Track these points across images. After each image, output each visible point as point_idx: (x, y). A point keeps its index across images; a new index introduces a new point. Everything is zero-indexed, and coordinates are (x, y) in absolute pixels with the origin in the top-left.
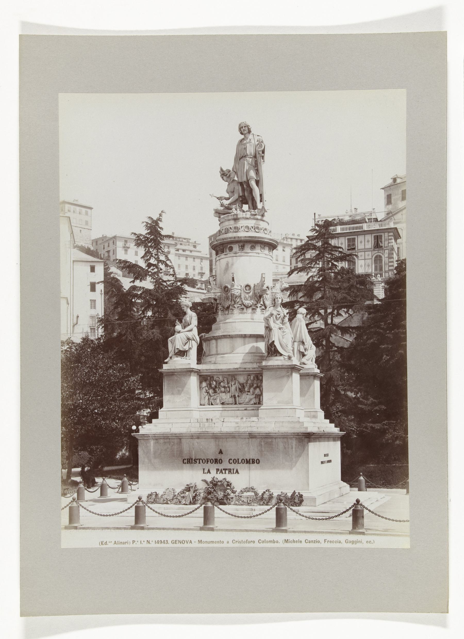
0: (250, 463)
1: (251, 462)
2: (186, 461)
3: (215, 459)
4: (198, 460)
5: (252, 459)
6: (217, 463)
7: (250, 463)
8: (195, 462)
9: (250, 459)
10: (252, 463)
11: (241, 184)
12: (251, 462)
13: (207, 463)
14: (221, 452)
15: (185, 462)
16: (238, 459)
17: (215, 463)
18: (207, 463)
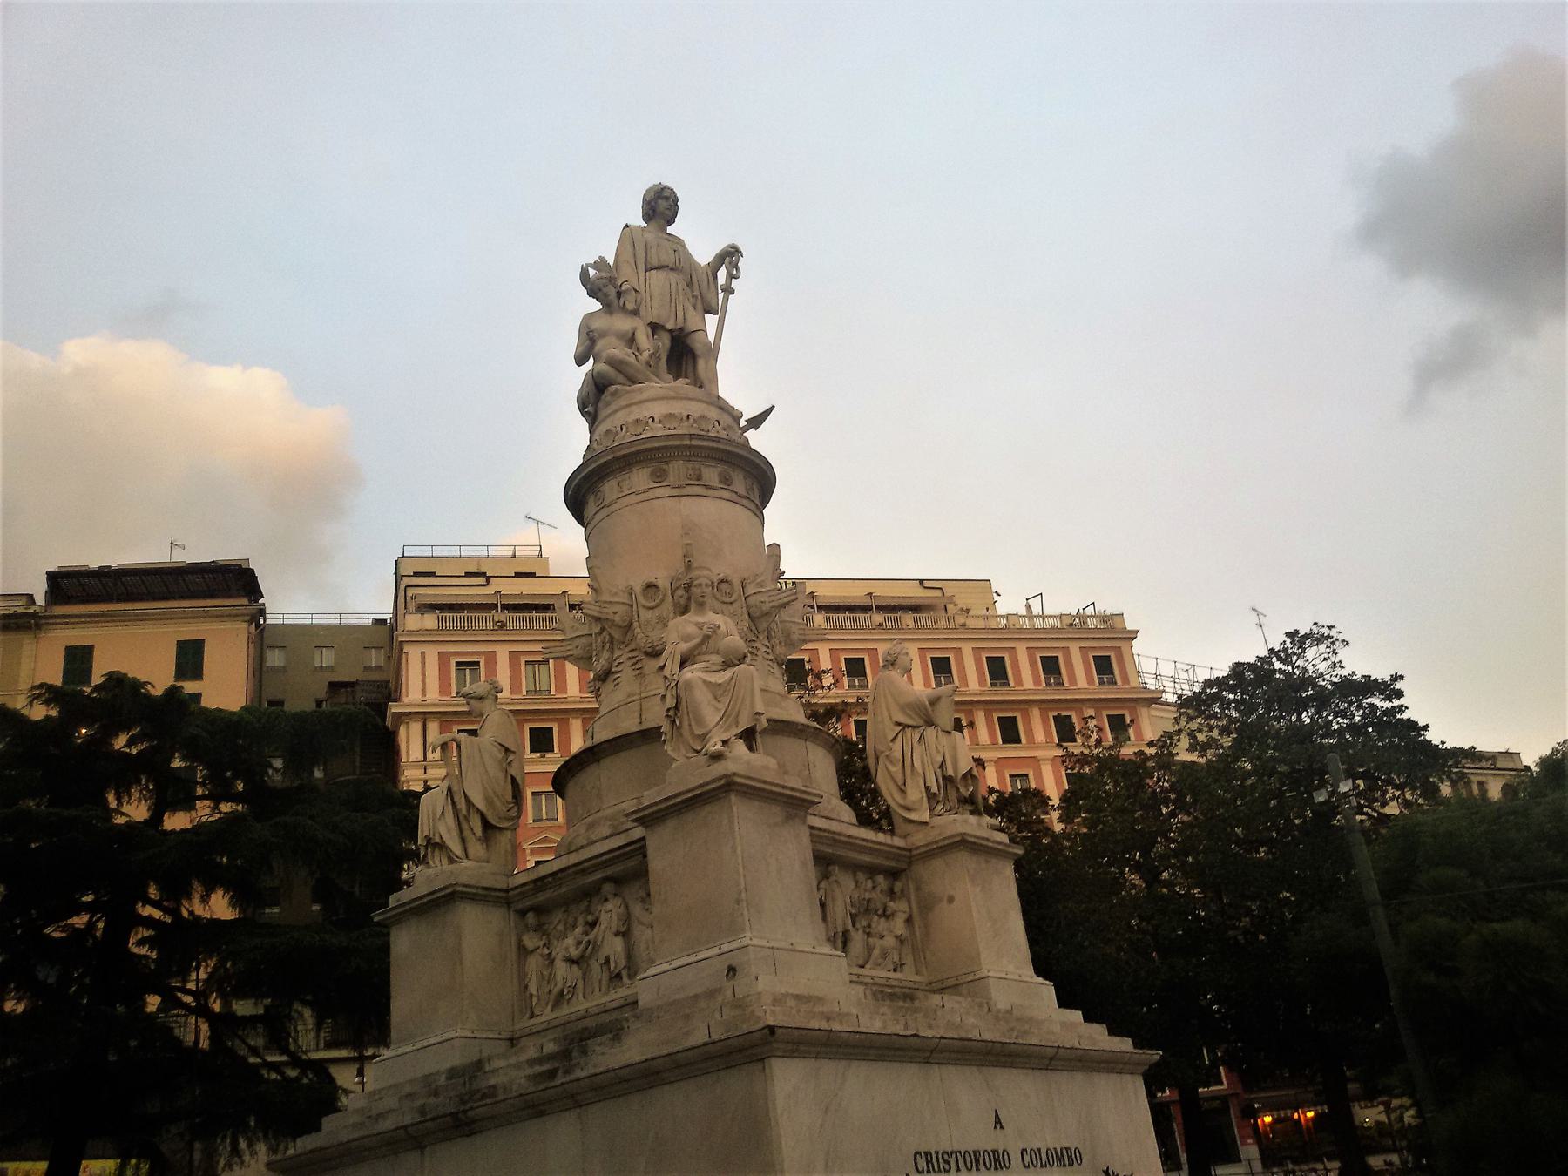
0: (1065, 1165)
1: (1067, 1162)
2: (922, 1163)
3: (993, 1151)
4: (954, 1156)
5: (1066, 1148)
6: (1002, 1168)
7: (1065, 1165)
8: (947, 1167)
9: (1061, 1150)
10: (1069, 1165)
11: (655, 328)
12: (1067, 1162)
13: (978, 1169)
14: (998, 1122)
15: (920, 1169)
16: (1039, 1150)
17: (996, 1169)
18: (978, 1169)
